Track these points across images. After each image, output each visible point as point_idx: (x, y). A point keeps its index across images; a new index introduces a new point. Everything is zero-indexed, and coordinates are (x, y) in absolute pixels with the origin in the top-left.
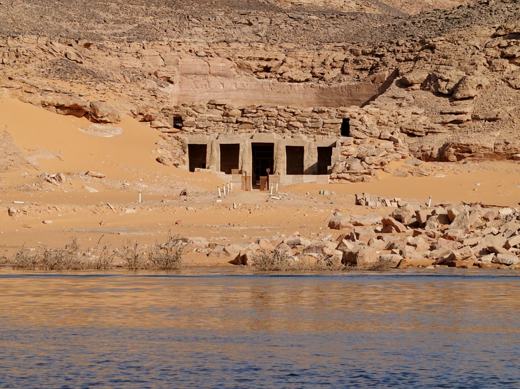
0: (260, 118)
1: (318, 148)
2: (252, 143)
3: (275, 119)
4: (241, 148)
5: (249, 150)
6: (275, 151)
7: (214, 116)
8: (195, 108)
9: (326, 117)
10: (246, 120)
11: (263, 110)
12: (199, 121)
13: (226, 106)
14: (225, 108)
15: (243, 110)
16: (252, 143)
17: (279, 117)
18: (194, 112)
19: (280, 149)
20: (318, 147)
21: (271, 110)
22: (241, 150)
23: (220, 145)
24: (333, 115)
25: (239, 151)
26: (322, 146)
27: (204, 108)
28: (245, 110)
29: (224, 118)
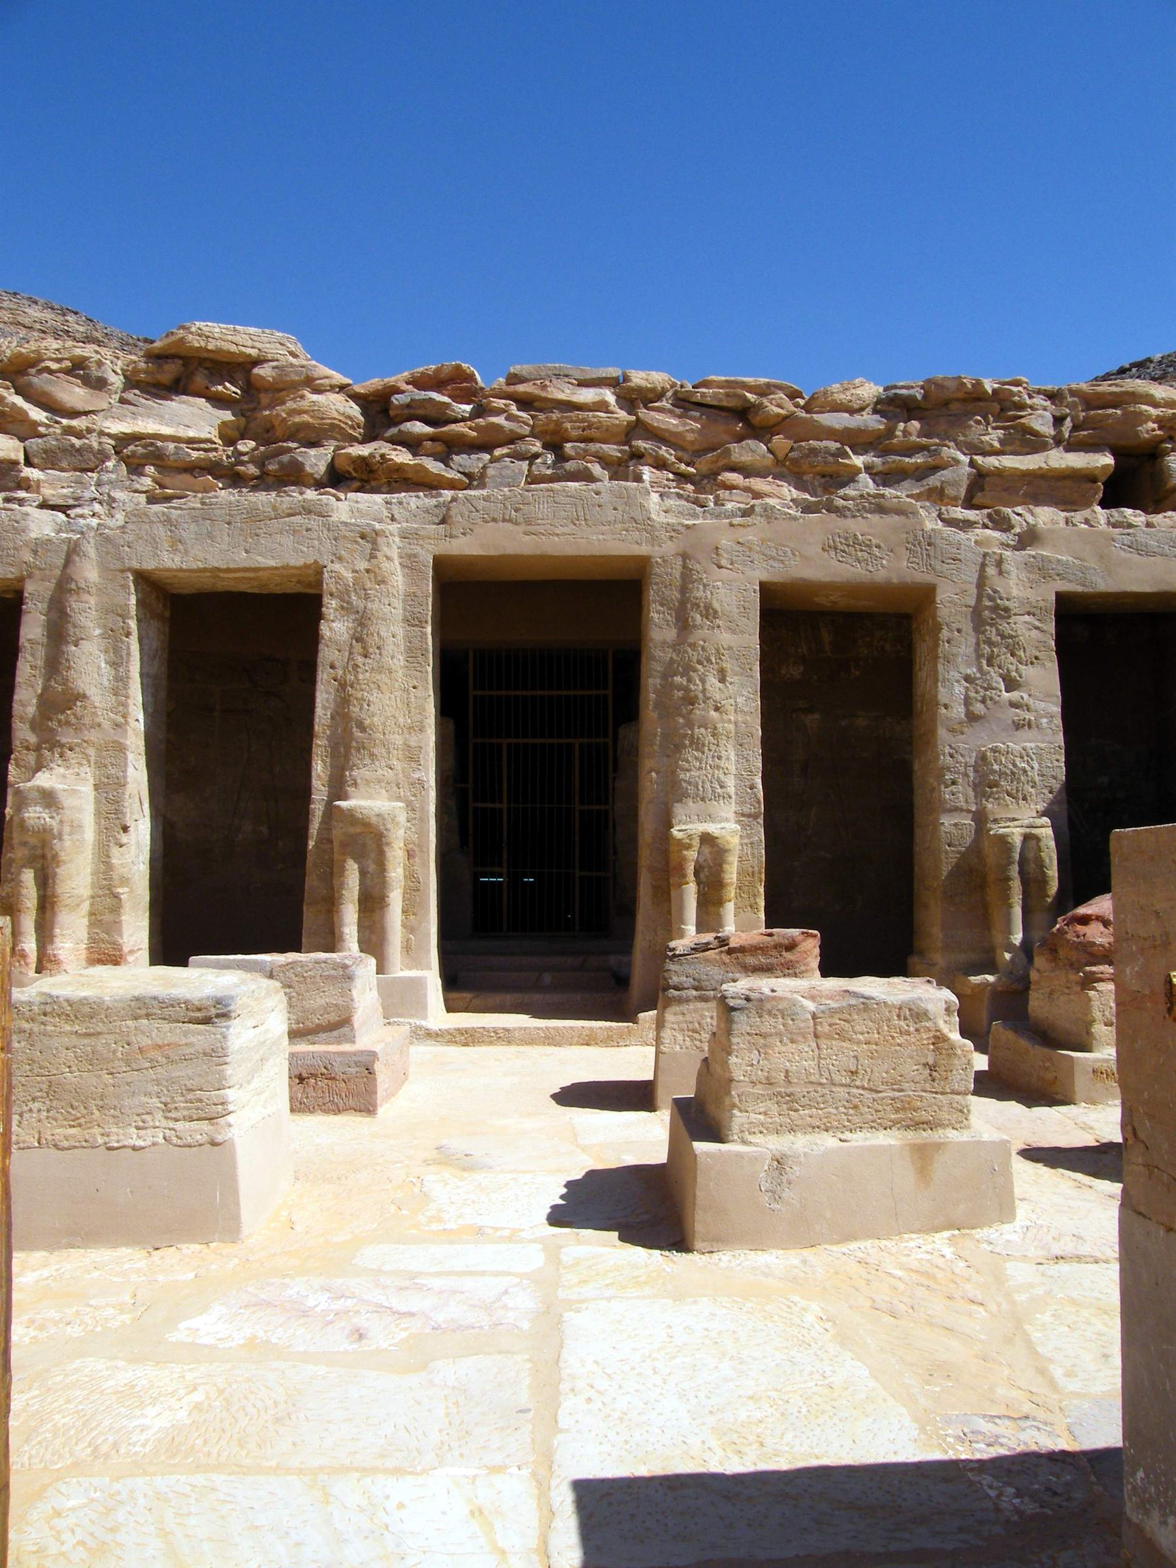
0: (498, 452)
1: (1061, 597)
2: (440, 564)
3: (612, 450)
4: (331, 605)
5: (412, 621)
6: (659, 627)
7: (166, 430)
8: (39, 381)
9: (993, 437)
10: (402, 457)
11: (525, 403)
12: (50, 460)
13: (264, 372)
14: (252, 388)
15: (379, 412)
16: (440, 564)
17: (642, 444)
18: (19, 401)
19: (709, 612)
20: (1062, 599)
21: (587, 395)
22: (335, 628)
23: (147, 582)
24: (1041, 421)
25: (313, 639)
26: (1103, 583)
27: (99, 384)
28: (397, 399)
29: (246, 446)
